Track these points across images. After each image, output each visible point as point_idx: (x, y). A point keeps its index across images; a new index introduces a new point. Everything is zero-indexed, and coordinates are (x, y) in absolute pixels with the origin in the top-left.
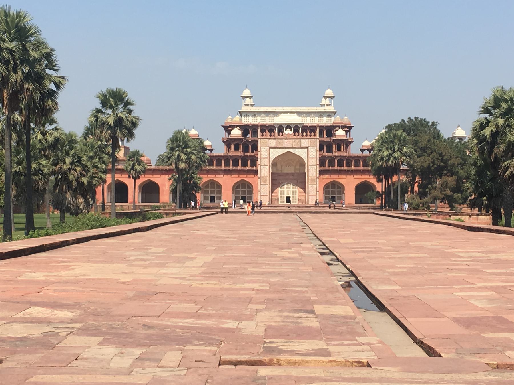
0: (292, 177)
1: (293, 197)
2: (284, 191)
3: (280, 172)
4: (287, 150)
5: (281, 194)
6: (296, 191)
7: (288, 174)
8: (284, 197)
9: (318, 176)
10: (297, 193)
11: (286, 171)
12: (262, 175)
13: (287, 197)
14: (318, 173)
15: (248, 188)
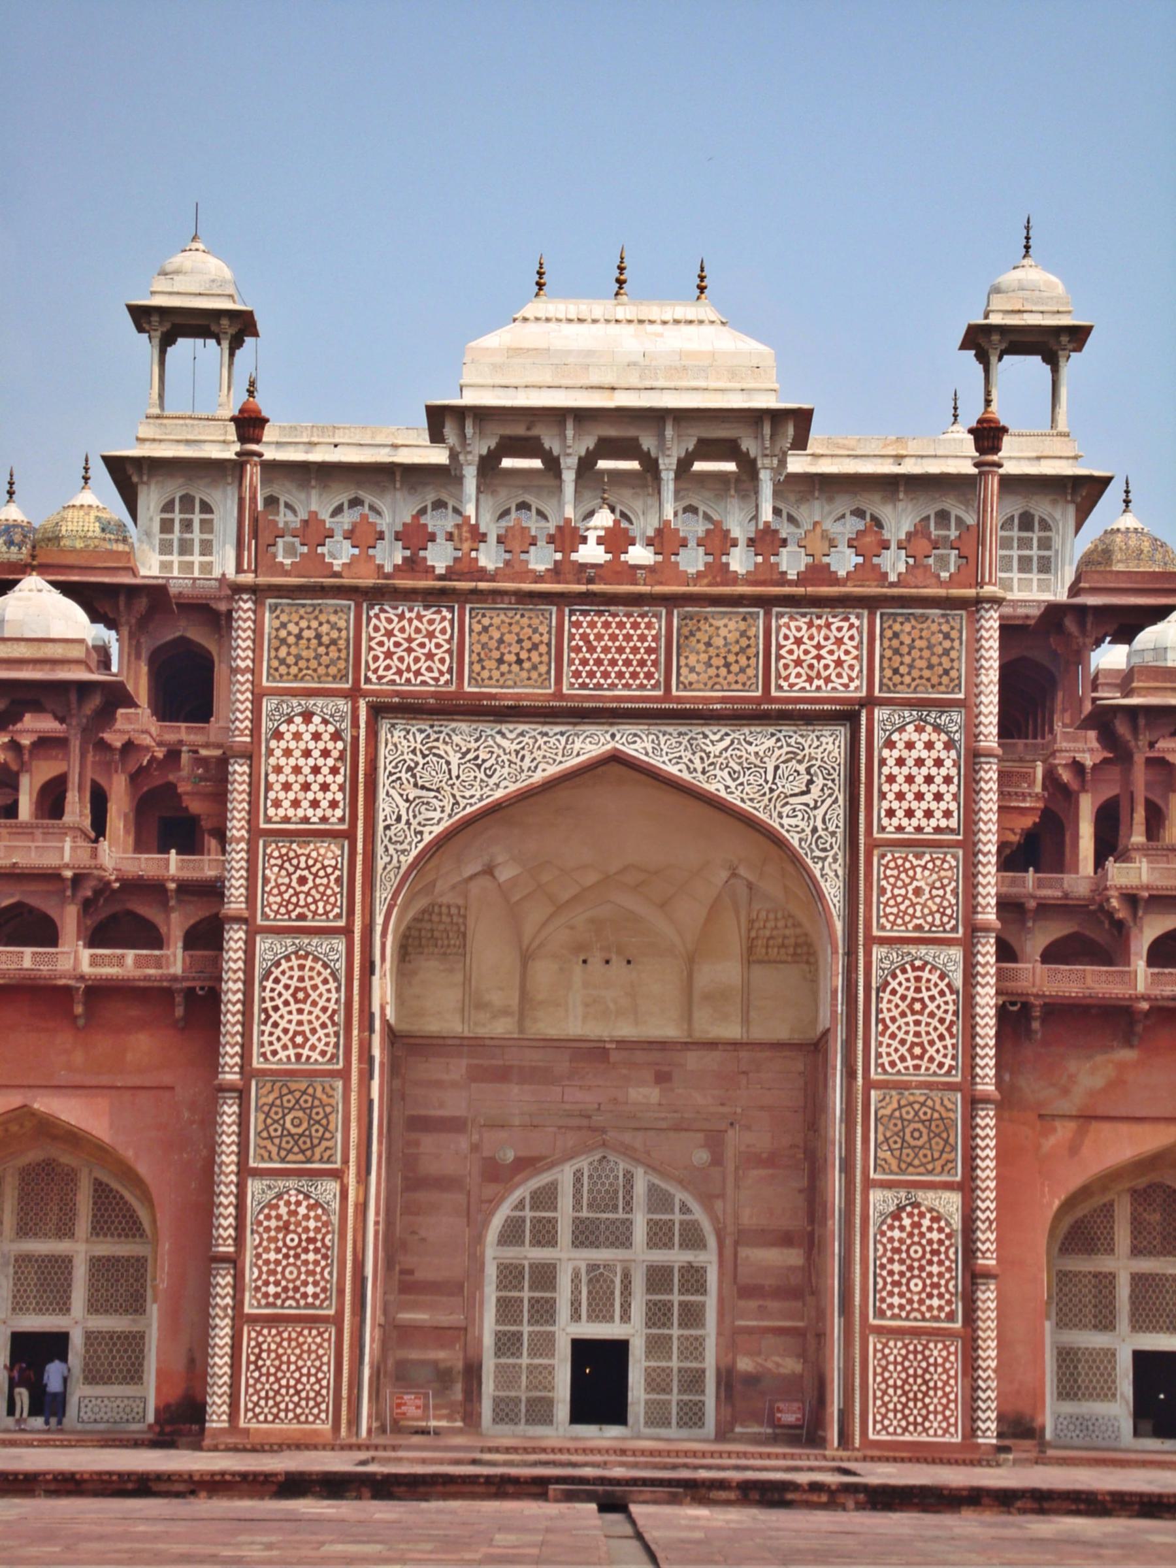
0: (644, 1094)
1: (657, 1346)
2: (545, 1276)
3: (502, 1027)
4: (590, 744)
5: (507, 1309)
6: (693, 1278)
7: (594, 1054)
8: (544, 1345)
9: (987, 1085)
10: (711, 1303)
11: (574, 1024)
12: (274, 1050)
13: (582, 1349)
14: (987, 1028)
15: (99, 1228)
